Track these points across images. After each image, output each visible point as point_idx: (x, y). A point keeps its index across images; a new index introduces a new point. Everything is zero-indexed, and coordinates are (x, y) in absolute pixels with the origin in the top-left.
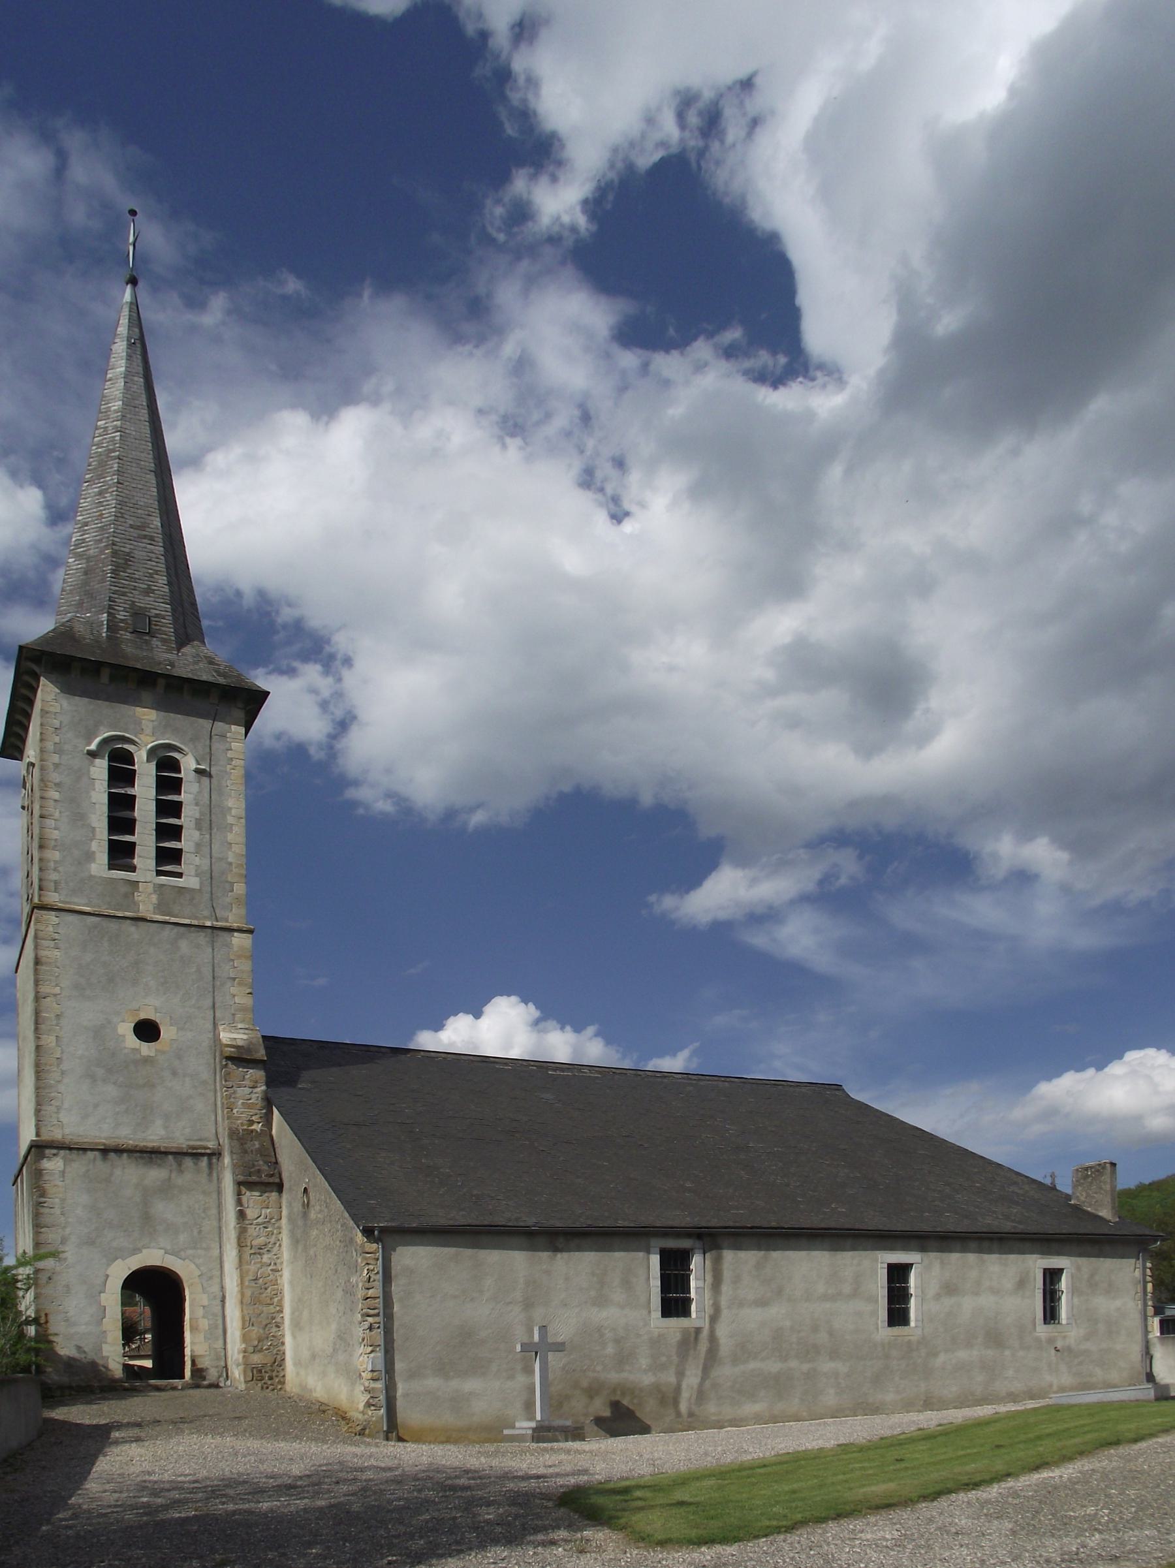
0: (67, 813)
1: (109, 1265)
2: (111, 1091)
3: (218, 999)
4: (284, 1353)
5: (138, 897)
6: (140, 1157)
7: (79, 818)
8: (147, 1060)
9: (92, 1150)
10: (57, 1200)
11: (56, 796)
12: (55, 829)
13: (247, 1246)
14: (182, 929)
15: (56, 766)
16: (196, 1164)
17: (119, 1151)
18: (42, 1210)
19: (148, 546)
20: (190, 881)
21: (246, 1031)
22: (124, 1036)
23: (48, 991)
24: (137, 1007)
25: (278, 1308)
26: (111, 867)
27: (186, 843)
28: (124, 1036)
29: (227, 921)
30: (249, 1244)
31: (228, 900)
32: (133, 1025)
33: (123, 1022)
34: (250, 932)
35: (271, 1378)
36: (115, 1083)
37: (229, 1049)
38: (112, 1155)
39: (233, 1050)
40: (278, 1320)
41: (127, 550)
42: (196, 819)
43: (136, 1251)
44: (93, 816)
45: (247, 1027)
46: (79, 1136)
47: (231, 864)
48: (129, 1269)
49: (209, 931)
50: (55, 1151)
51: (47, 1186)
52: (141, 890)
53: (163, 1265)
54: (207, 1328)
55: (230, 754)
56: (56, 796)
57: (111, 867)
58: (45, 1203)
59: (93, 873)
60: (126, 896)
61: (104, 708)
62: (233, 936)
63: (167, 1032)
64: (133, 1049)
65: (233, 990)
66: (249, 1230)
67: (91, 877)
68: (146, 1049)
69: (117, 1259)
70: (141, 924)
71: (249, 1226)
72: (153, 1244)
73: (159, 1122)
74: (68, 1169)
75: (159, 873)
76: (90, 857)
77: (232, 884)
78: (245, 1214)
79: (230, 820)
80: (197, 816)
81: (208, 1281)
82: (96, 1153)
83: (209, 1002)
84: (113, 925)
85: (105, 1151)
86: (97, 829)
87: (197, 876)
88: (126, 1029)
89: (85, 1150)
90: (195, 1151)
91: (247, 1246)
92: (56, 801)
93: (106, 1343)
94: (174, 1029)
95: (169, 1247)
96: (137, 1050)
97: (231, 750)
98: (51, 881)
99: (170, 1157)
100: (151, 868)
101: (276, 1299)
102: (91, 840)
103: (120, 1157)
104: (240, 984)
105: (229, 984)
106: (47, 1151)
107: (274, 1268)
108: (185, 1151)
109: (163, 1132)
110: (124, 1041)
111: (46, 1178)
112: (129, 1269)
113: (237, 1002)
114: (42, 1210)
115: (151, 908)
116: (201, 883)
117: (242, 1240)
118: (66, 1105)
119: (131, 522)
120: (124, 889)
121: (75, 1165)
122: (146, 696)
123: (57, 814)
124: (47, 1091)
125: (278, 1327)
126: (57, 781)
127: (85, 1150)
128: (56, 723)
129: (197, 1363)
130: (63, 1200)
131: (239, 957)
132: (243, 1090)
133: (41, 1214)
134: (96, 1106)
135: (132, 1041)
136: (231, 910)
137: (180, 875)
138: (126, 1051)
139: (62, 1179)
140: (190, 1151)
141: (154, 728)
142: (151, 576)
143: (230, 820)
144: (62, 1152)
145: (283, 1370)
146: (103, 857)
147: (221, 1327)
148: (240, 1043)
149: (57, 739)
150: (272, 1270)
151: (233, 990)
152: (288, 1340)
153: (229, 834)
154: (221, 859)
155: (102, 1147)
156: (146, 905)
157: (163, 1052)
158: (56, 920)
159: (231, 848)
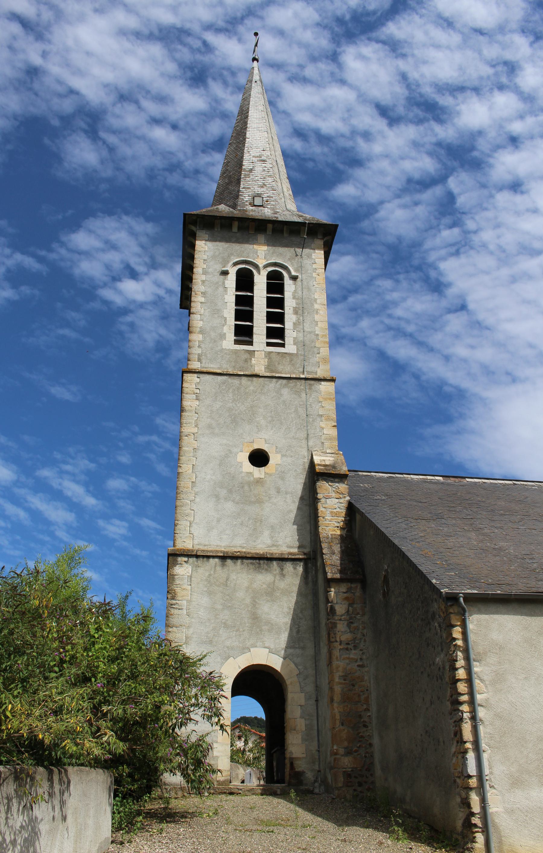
0: (209, 310)
1: (222, 664)
2: (229, 506)
3: (311, 432)
4: (372, 756)
5: (254, 361)
6: (251, 563)
7: (217, 312)
8: (259, 482)
9: (214, 557)
10: (185, 602)
11: (203, 300)
12: (200, 320)
13: (336, 641)
14: (284, 381)
15: (203, 282)
16: (295, 569)
17: (234, 558)
18: (173, 611)
19: (263, 164)
20: (290, 347)
21: (333, 455)
22: (241, 463)
23: (189, 431)
24: (251, 440)
25: (365, 707)
26: (237, 342)
27: (289, 324)
28: (241, 463)
29: (316, 373)
30: (338, 640)
31: (317, 359)
32: (248, 454)
33: (242, 451)
34: (333, 380)
35: (360, 784)
36: (233, 501)
37: (320, 467)
38: (229, 561)
39: (322, 467)
40: (366, 719)
41: (251, 168)
42: (293, 307)
43: (245, 649)
44: (225, 310)
45: (333, 452)
46: (205, 546)
47: (317, 335)
48: (240, 667)
49: (303, 381)
50: (186, 559)
51: (178, 590)
52: (256, 356)
53: (267, 664)
54: (304, 730)
55: (314, 266)
56: (203, 300)
57: (237, 342)
58: (174, 604)
59: (224, 347)
60: (246, 361)
61: (236, 247)
62: (321, 384)
63: (274, 459)
64: (248, 473)
65: (322, 424)
66: (338, 625)
67: (222, 350)
68: (258, 472)
69: (229, 657)
70: (255, 379)
71: (338, 622)
72: (258, 644)
73: (267, 533)
74: (195, 574)
75: (269, 344)
76: (223, 336)
77: (319, 348)
78: (335, 610)
79: (316, 306)
80: (295, 305)
81: (305, 679)
82: (217, 560)
83: (303, 435)
84: (235, 381)
85: (224, 558)
86: (227, 319)
87: (294, 344)
88: (244, 457)
89: (208, 557)
90: (293, 557)
91: (336, 641)
92: (201, 303)
93: (217, 742)
94: (279, 456)
95: (272, 646)
96: (251, 473)
97: (316, 263)
98: (196, 354)
99: (275, 563)
100: (263, 342)
101: (363, 697)
102: (224, 326)
103: (235, 563)
104: (326, 420)
105: (319, 419)
106: (180, 559)
107: (361, 663)
108: (287, 557)
109: (269, 542)
110: (241, 467)
111: (177, 582)
112: (240, 667)
113: (325, 433)
114: (173, 611)
115: (263, 369)
116: (298, 349)
117: (332, 635)
118: (197, 520)
119: (254, 155)
120: (247, 356)
121: (201, 570)
122: (261, 238)
123: (202, 311)
124: (183, 508)
125: (365, 726)
126: (202, 291)
127: (208, 557)
128: (205, 257)
129: (295, 765)
130: (189, 602)
131: (325, 399)
132: (332, 501)
133: (171, 615)
134: (218, 521)
135: (248, 467)
136: (319, 367)
137: (283, 345)
138: (243, 475)
139: (189, 583)
140: (290, 557)
141: (265, 255)
142: (264, 178)
143: (316, 306)
144: (191, 560)
145: (372, 775)
146: (231, 336)
147: (316, 728)
148: (327, 463)
149: (205, 266)
150: (358, 666)
151: (322, 424)
152: (376, 741)
153: (315, 315)
154: (310, 333)
155: (222, 555)
156: (259, 367)
157: (271, 475)
158: (198, 380)
159: (317, 324)
